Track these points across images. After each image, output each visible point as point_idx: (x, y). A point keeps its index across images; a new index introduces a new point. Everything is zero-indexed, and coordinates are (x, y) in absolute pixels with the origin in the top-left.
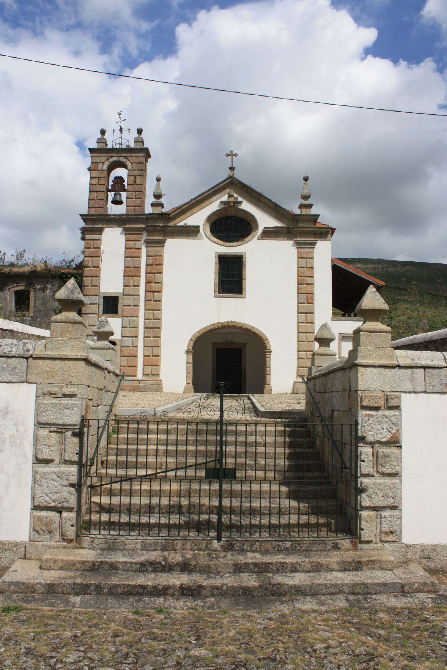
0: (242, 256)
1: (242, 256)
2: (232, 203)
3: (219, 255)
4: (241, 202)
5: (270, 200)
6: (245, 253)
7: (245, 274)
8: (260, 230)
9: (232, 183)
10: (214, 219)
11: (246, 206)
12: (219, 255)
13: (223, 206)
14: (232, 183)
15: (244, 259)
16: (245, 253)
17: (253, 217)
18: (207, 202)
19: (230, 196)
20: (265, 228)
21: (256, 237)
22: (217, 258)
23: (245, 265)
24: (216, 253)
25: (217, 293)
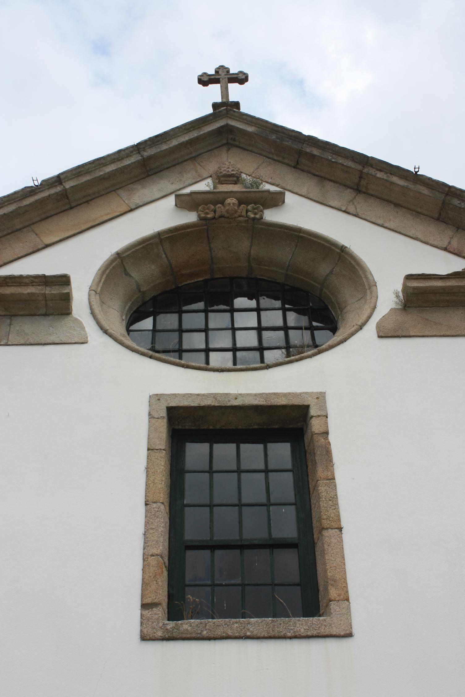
0: (307, 408)
1: (307, 408)
2: (231, 201)
3: (170, 410)
4: (276, 201)
5: (415, 178)
6: (321, 397)
7: (334, 499)
8: (387, 295)
9: (227, 131)
10: (146, 274)
11: (302, 212)
12: (170, 410)
13: (190, 218)
14: (227, 131)
15: (316, 425)
16: (321, 397)
17: (340, 257)
18: (114, 204)
19: (220, 178)
20: (409, 277)
21: (371, 328)
22: (163, 426)
23: (328, 452)
24: (156, 398)
25: (160, 613)
